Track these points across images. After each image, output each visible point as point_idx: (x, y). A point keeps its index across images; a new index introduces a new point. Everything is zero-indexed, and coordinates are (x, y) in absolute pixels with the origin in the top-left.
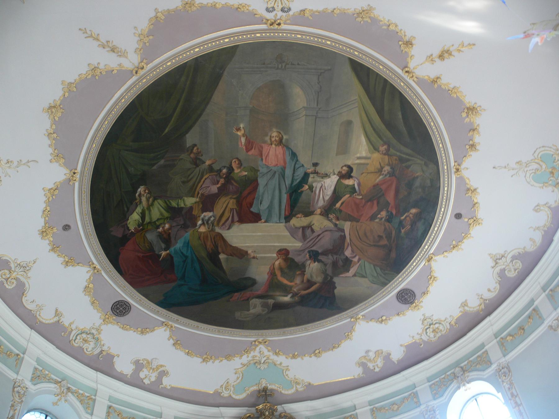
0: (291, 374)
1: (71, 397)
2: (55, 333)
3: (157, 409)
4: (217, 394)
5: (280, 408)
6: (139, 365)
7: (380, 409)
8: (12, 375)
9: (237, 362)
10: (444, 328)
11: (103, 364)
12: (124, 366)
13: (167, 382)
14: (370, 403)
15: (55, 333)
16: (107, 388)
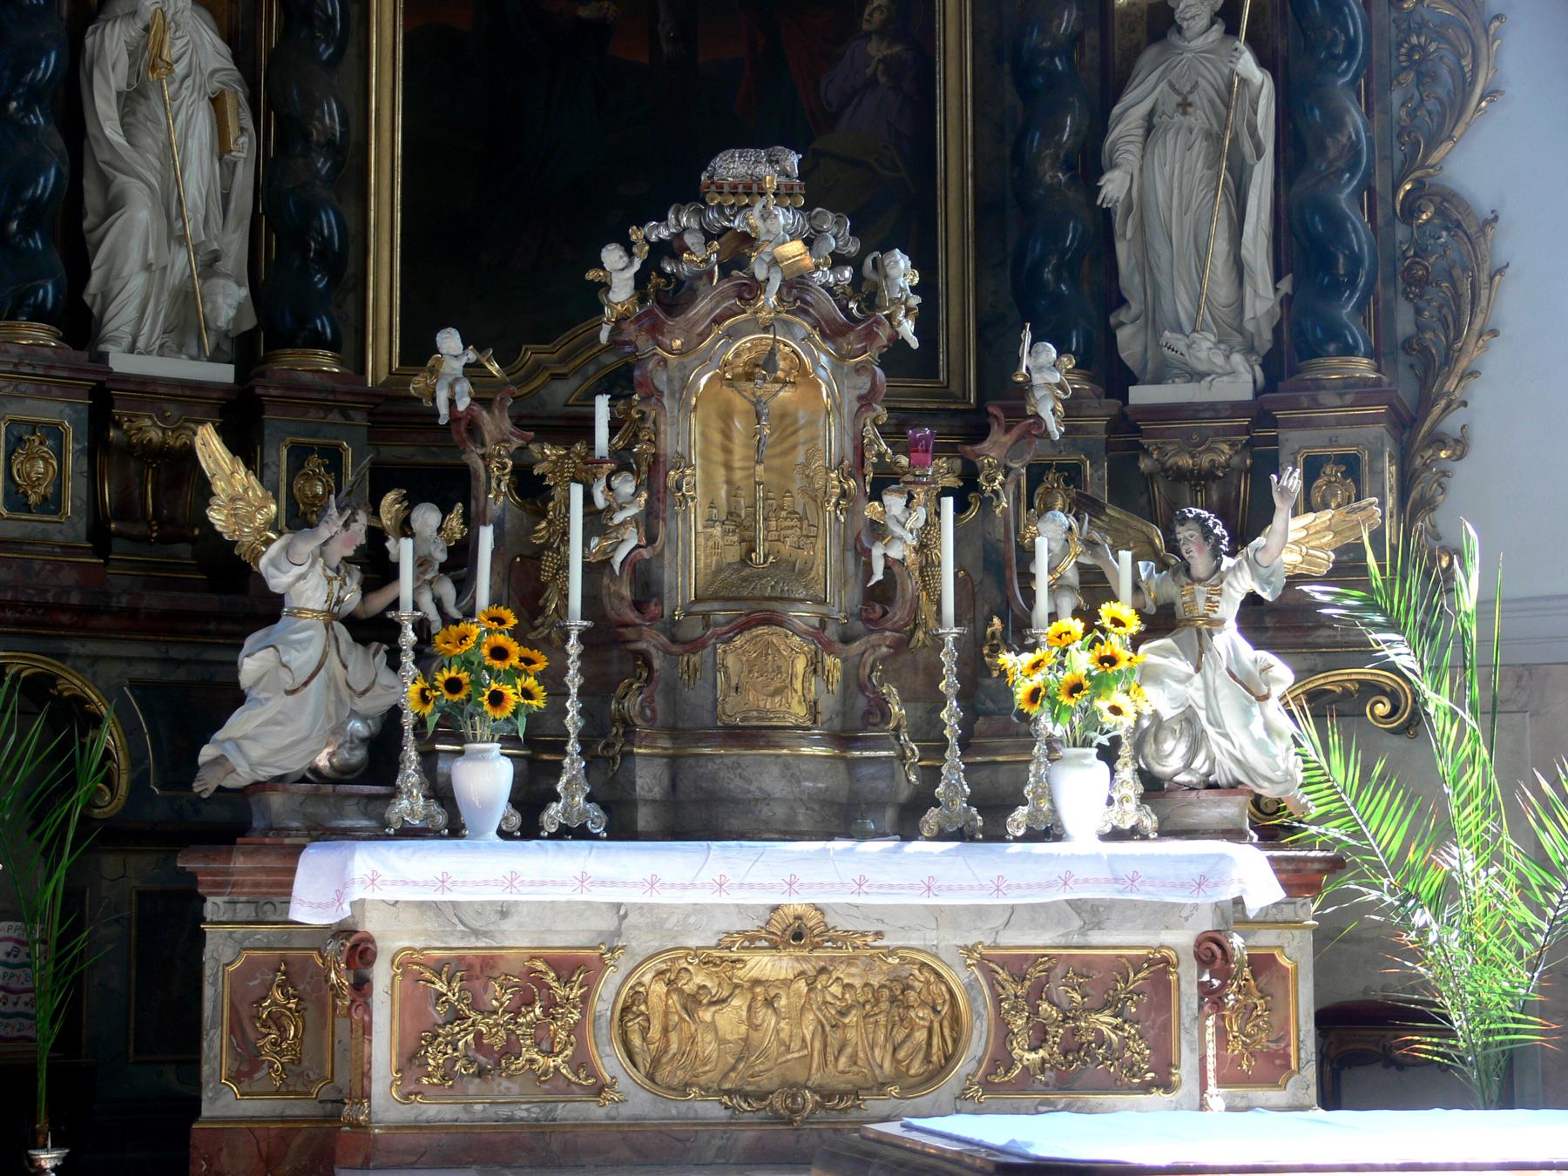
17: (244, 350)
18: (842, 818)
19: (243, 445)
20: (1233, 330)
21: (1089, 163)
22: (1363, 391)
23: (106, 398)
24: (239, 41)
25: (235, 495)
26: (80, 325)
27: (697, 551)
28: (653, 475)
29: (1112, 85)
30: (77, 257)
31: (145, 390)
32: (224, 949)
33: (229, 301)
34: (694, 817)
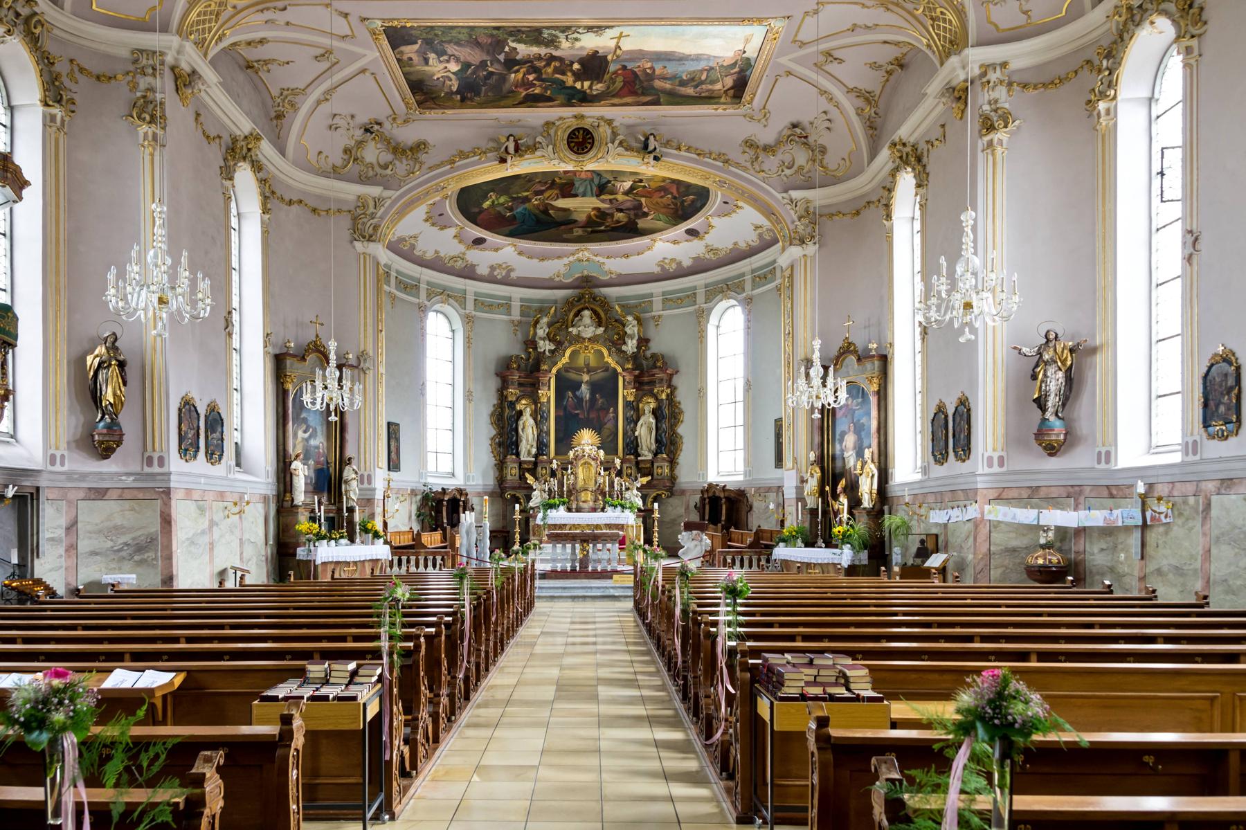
0: (606, 268)
1: (451, 300)
2: (436, 264)
3: (507, 294)
4: (551, 279)
5: (596, 290)
6: (492, 268)
7: (671, 300)
8: (416, 301)
9: (566, 260)
10: (722, 254)
11: (468, 273)
12: (483, 270)
13: (513, 275)
14: (664, 294)
15: (436, 264)
16: (472, 286)
17: (536, 456)
18: (594, 510)
19: (534, 475)
20: (650, 450)
21: (634, 431)
22: (664, 459)
23: (521, 463)
24: (535, 419)
25: (530, 480)
26: (518, 454)
27: (580, 483)
28: (575, 475)
29: (638, 419)
30: (517, 447)
31: (525, 462)
32: (531, 524)
33: (534, 451)
34: (579, 510)
